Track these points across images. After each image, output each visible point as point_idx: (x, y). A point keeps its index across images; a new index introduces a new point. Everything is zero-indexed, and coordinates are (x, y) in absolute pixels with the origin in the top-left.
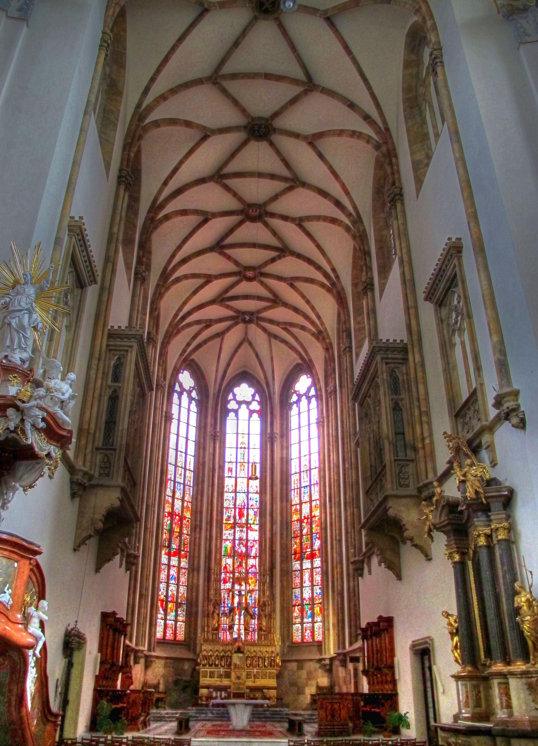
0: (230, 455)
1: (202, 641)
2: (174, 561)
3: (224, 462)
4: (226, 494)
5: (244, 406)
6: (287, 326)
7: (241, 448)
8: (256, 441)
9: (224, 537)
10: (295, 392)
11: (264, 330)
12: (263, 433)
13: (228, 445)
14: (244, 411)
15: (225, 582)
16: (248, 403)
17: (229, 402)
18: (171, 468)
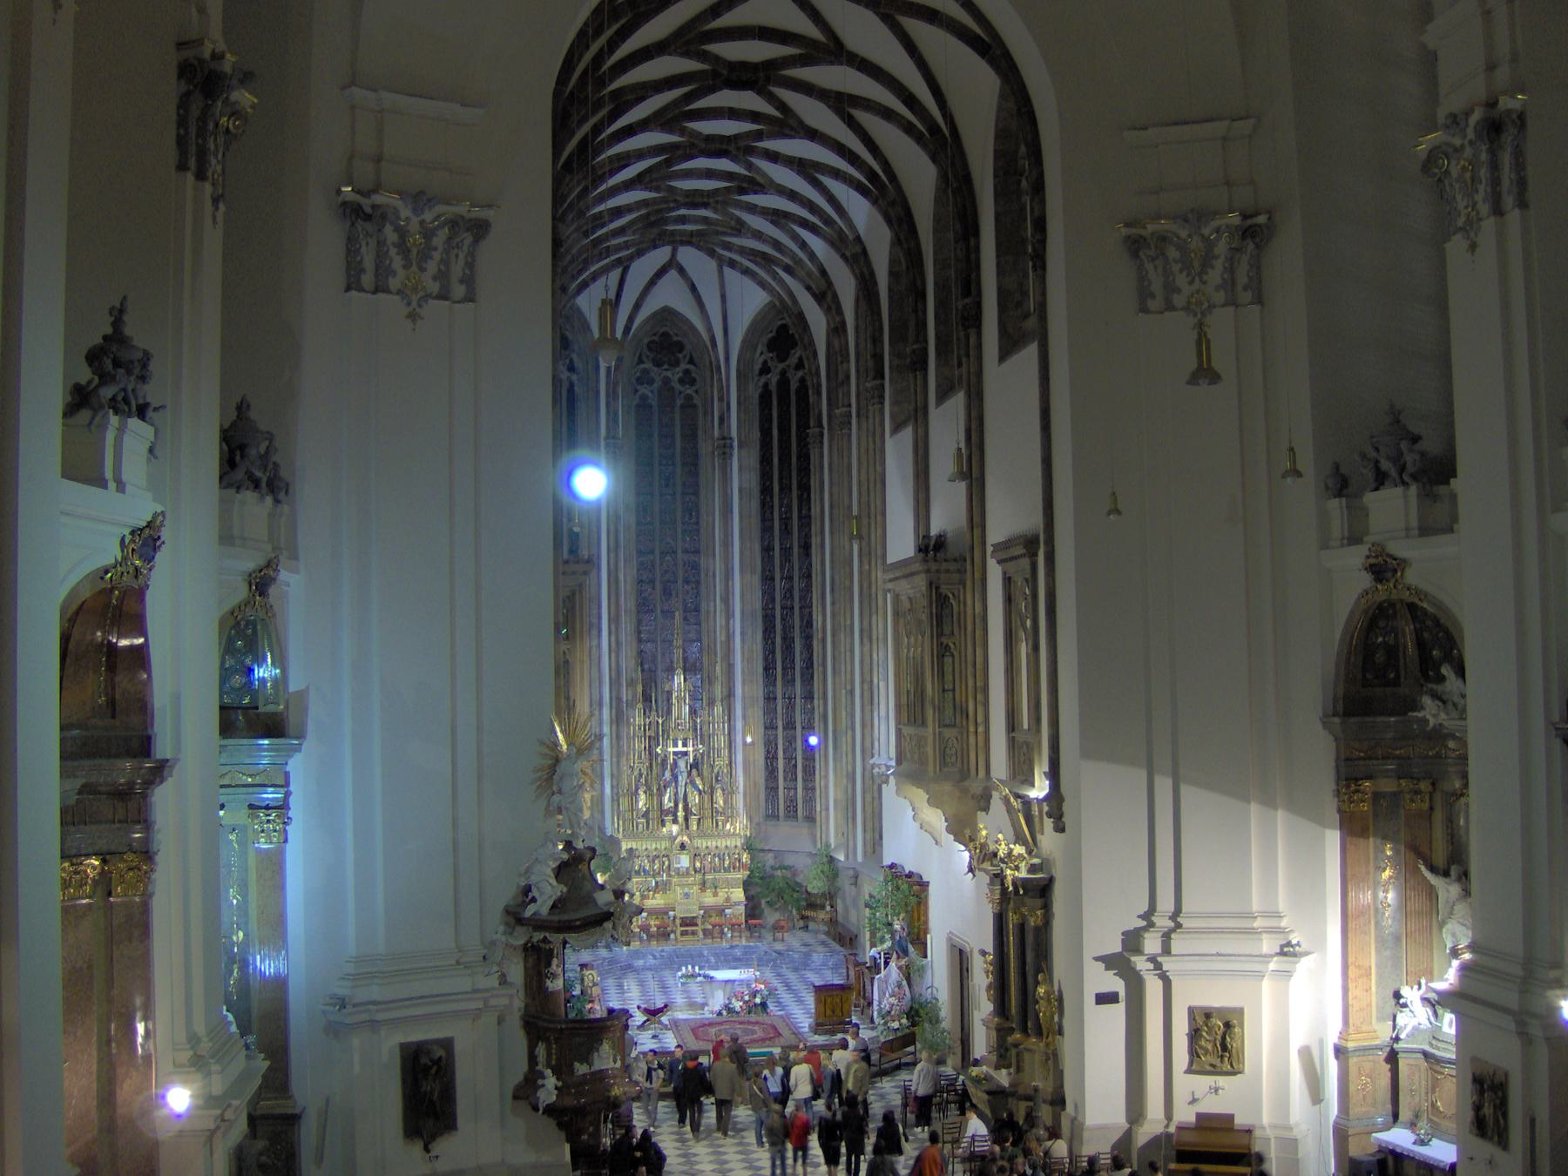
11: (711, 253)
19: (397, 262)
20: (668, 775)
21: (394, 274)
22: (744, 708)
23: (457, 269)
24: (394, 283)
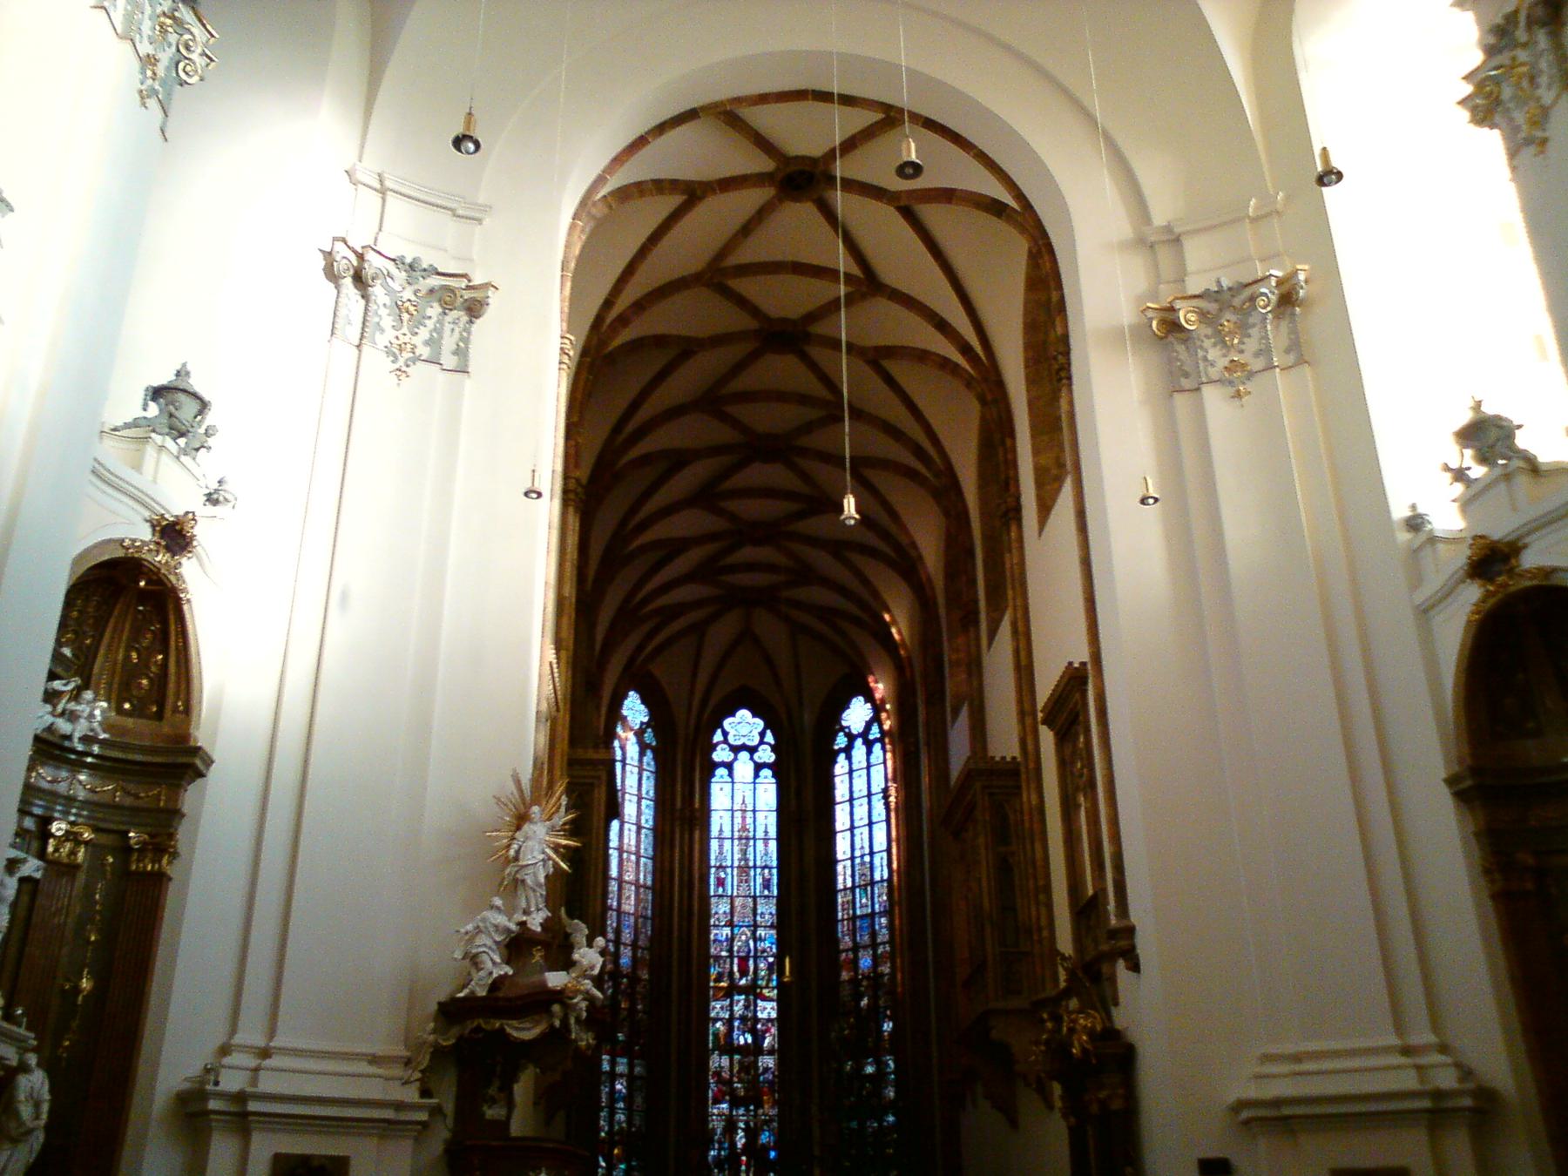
0: (722, 850)
2: (621, 1068)
3: (709, 867)
4: (714, 932)
5: (744, 755)
6: (827, 614)
7: (740, 838)
8: (768, 822)
9: (713, 1015)
10: (842, 729)
12: (782, 810)
13: (714, 832)
14: (744, 766)
15: (717, 1101)
16: (753, 750)
17: (714, 747)
18: (613, 886)
19: (388, 322)
21: (382, 331)
23: (449, 343)
24: (382, 340)
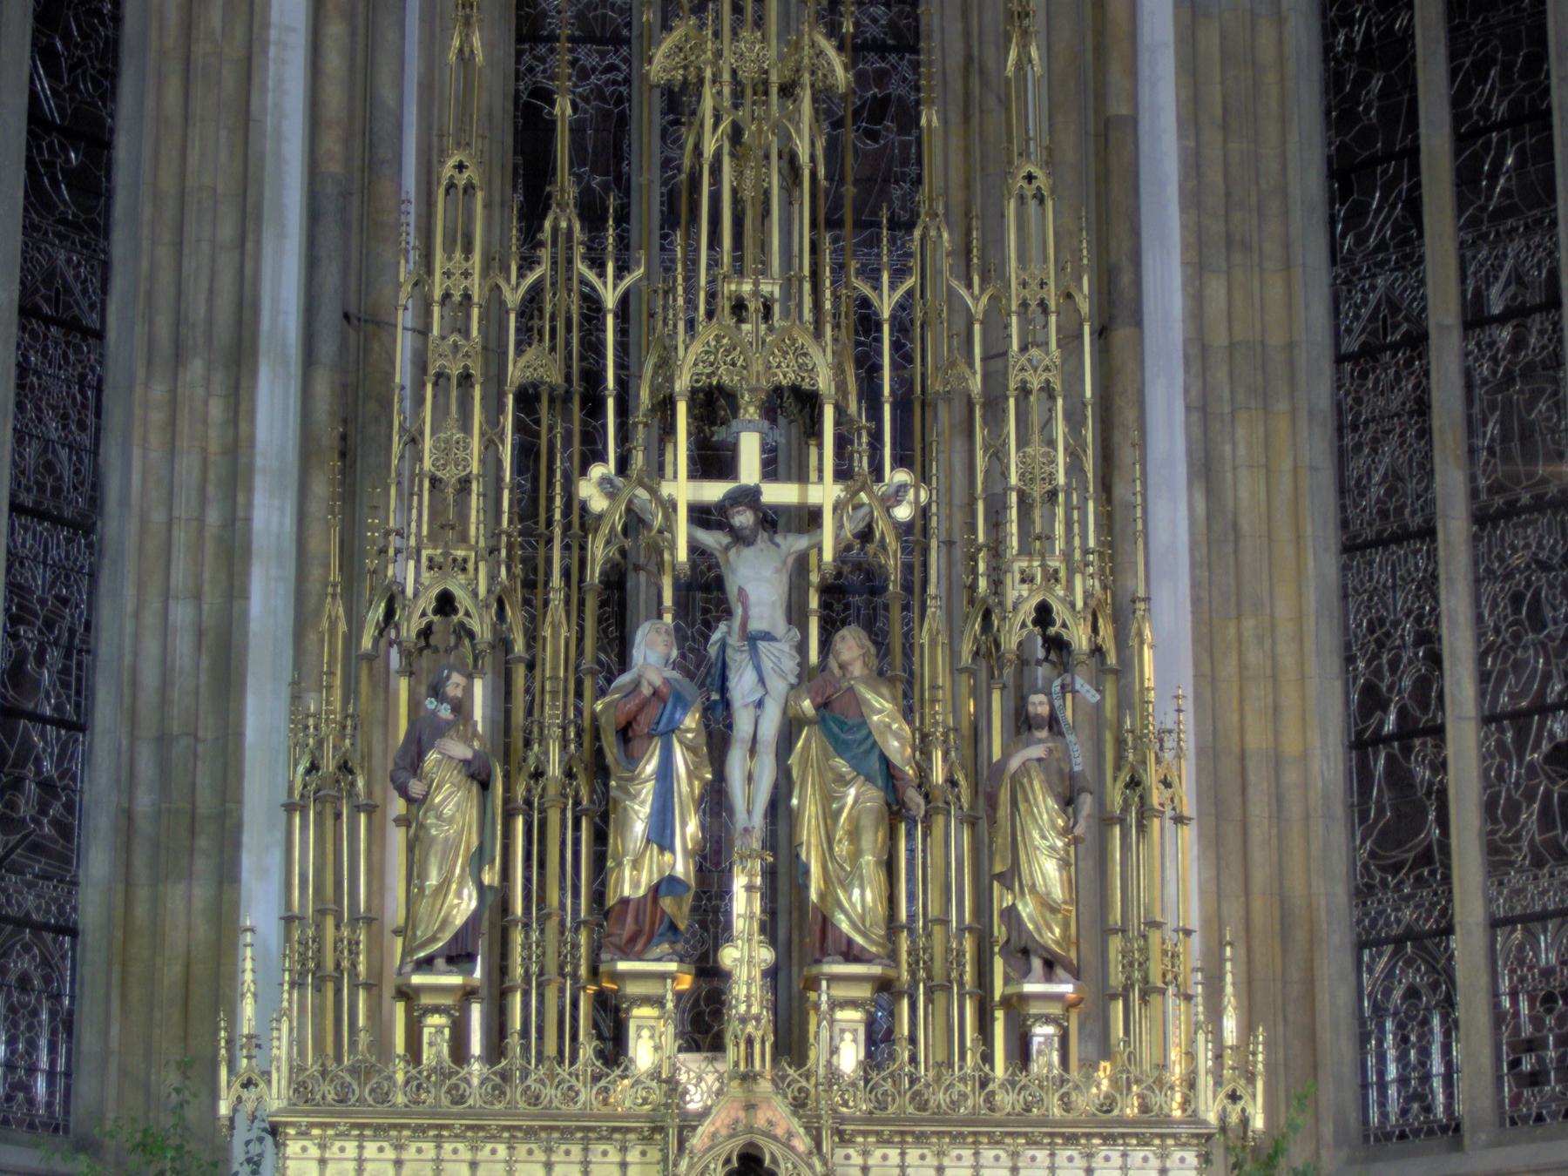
1: (276, 1096)
20: (652, 652)
22: (1202, 410)
